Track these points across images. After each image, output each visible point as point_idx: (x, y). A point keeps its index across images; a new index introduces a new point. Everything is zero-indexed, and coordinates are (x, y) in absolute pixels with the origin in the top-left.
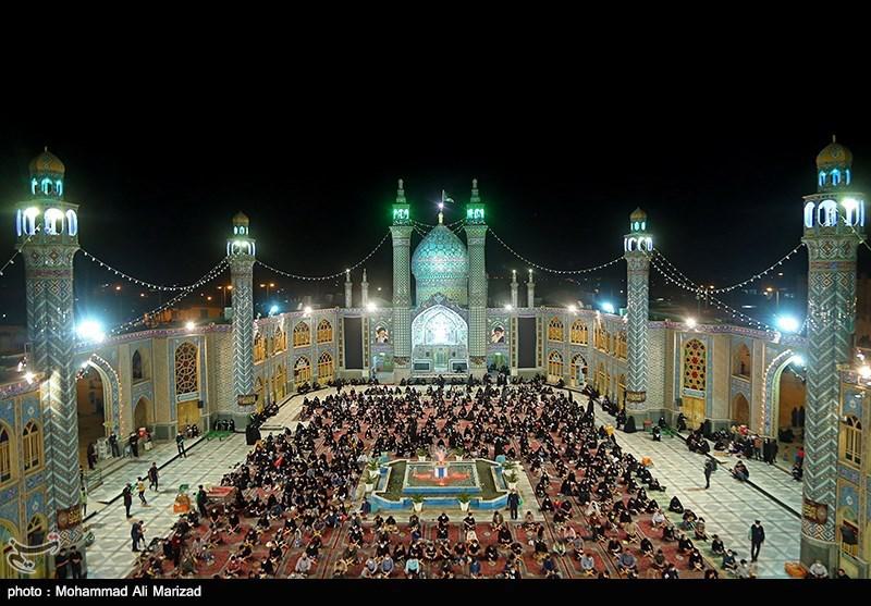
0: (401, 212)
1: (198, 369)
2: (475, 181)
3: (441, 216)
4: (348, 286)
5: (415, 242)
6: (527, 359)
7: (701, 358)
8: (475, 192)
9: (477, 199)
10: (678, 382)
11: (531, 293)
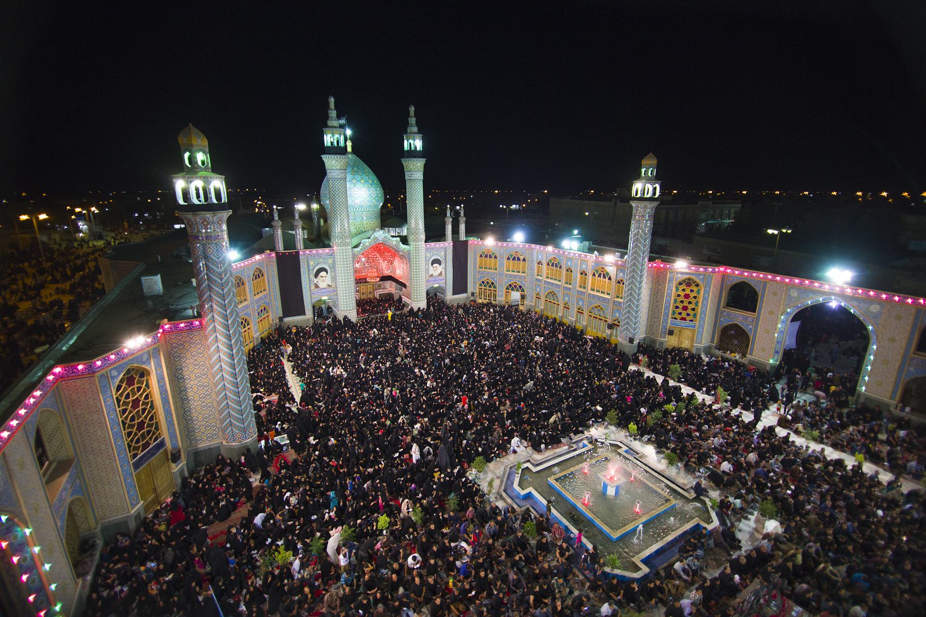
1: (158, 402)
2: (412, 109)
6: (460, 285)
7: (692, 295)
8: (413, 120)
9: (415, 129)
10: (667, 315)
11: (462, 227)
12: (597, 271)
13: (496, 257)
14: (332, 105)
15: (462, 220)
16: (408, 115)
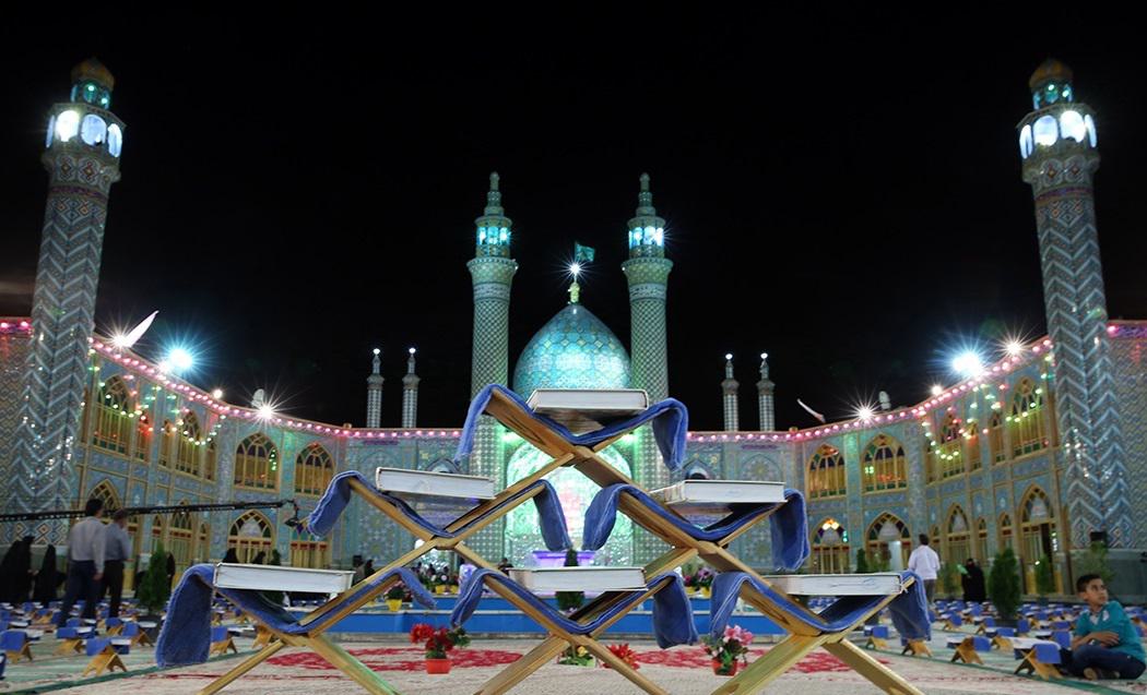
0: (494, 234)
2: (645, 178)
3: (574, 290)
4: (376, 380)
5: (521, 336)
9: (649, 210)
11: (766, 403)
12: (1017, 397)
13: (841, 462)
14: (495, 184)
15: (765, 385)
16: (638, 189)
